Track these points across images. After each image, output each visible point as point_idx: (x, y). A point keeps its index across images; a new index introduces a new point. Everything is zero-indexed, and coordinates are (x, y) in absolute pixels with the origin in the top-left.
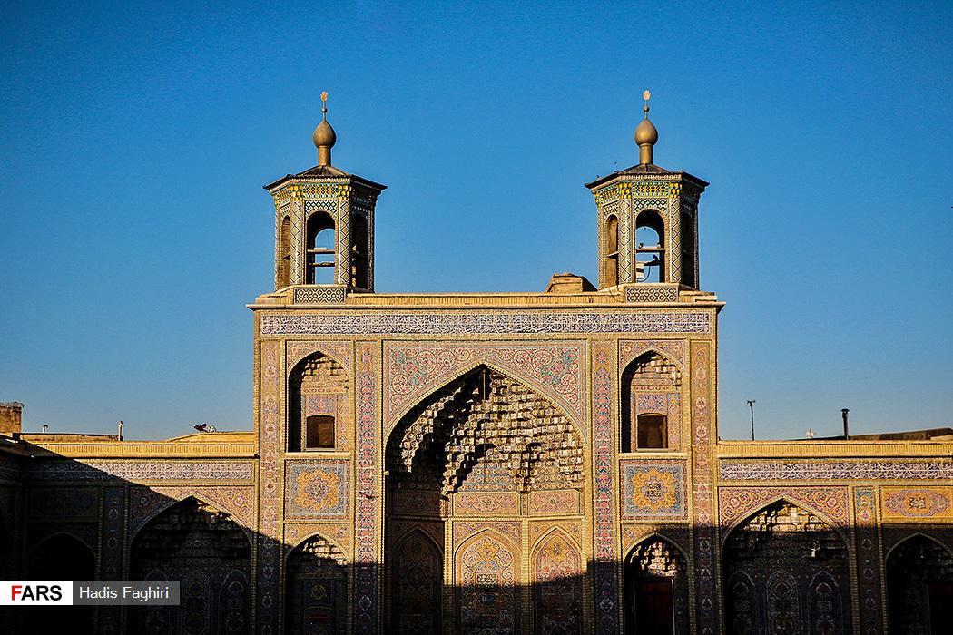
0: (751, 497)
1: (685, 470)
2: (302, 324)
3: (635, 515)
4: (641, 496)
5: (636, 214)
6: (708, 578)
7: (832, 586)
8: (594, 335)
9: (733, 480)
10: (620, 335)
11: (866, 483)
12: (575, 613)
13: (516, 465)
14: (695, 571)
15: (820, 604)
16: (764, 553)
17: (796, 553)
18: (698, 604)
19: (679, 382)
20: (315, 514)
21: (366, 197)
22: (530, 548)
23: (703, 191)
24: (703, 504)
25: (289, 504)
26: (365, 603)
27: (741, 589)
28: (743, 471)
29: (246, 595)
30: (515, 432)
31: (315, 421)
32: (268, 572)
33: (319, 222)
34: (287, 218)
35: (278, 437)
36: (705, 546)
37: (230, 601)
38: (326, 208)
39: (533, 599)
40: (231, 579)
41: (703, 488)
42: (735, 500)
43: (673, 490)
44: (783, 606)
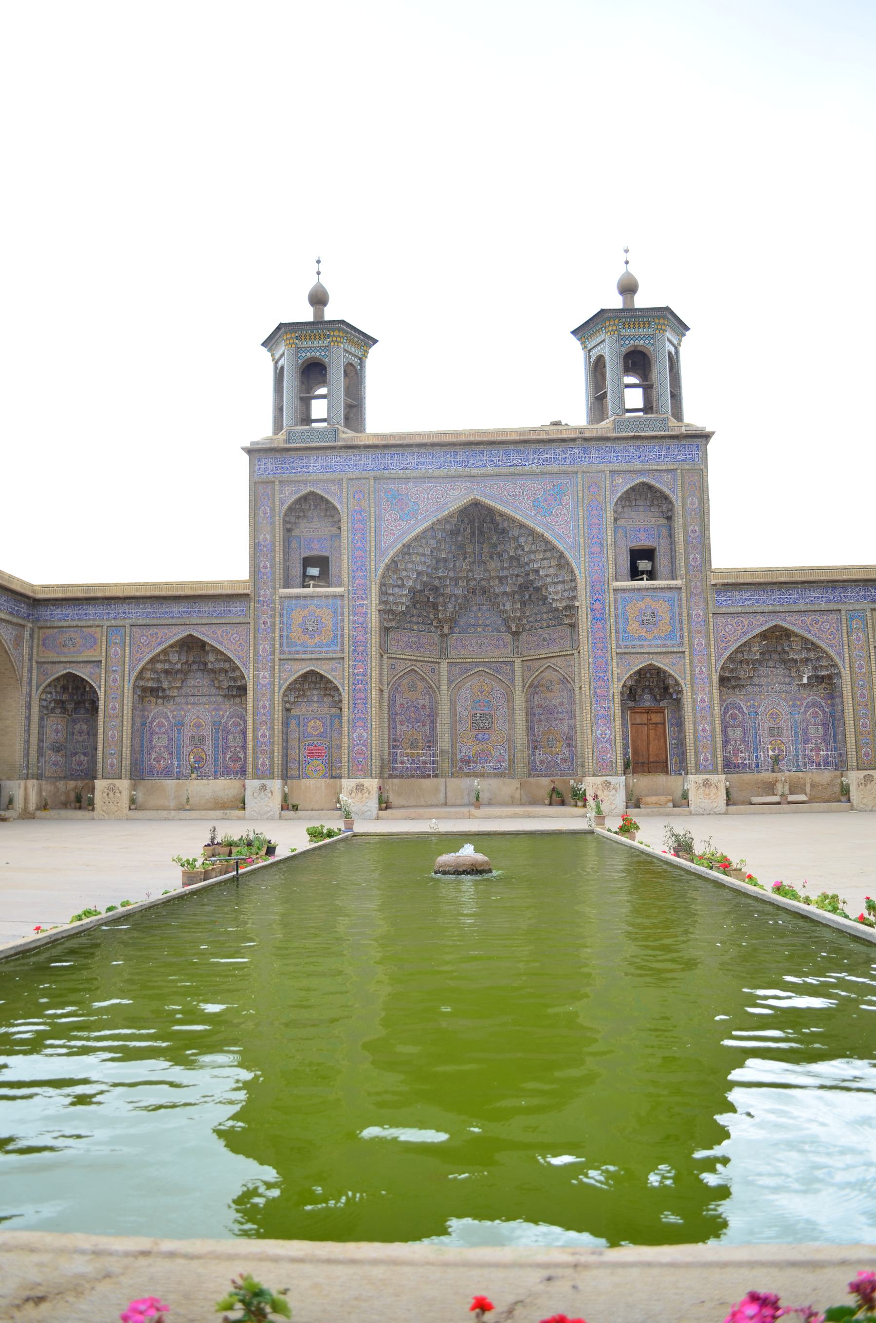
0: (746, 623)
1: (680, 599)
2: (294, 465)
3: (630, 643)
4: (635, 625)
5: (624, 350)
6: (705, 705)
7: (824, 712)
8: (584, 466)
9: (728, 606)
10: (612, 467)
11: (858, 607)
12: (568, 745)
13: (508, 606)
14: (692, 698)
15: (811, 730)
16: (756, 681)
17: (787, 680)
18: (696, 731)
19: (670, 514)
20: (309, 649)
21: (358, 345)
22: (524, 687)
23: (685, 335)
24: (699, 632)
25: (284, 640)
26: (360, 736)
27: (734, 717)
28: (738, 597)
29: (244, 733)
30: (505, 573)
31: (308, 562)
32: (264, 707)
33: (313, 372)
34: (282, 368)
35: (274, 573)
36: (701, 673)
37: (230, 737)
38: (318, 354)
39: (527, 735)
40: (230, 717)
41: (698, 616)
42: (730, 627)
43: (668, 618)
44: (775, 732)
